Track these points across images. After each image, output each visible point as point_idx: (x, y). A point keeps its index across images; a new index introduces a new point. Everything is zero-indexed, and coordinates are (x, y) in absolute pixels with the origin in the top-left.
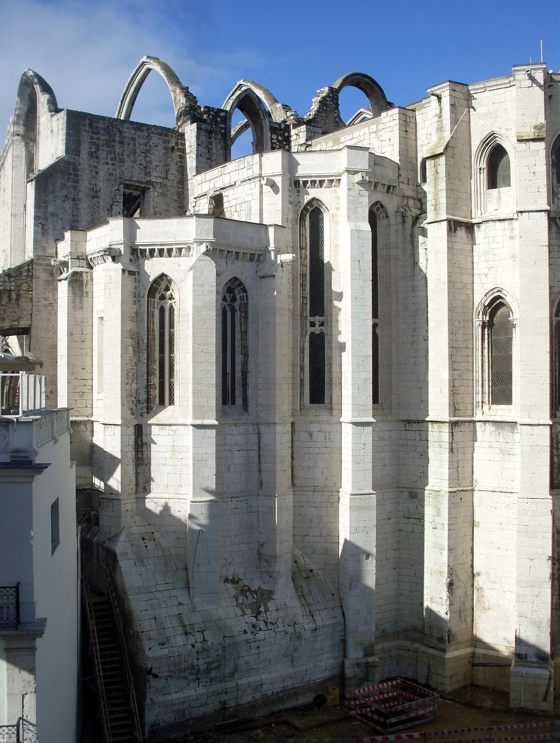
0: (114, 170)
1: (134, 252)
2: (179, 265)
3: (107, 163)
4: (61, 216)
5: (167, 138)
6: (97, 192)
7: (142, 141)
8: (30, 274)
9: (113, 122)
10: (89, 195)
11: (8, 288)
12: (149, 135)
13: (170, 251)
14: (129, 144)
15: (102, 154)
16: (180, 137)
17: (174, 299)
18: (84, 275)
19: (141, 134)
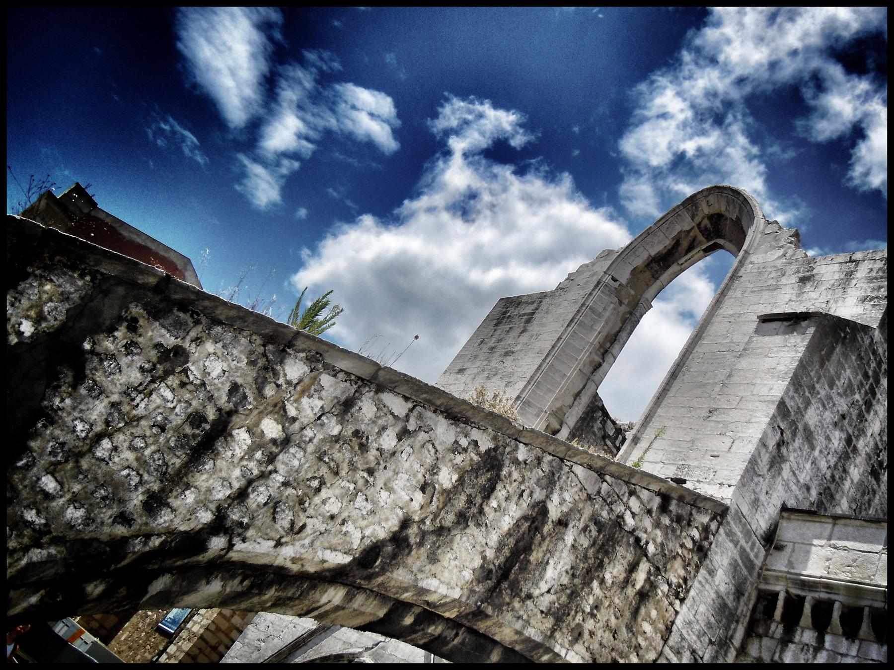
4: (817, 453)
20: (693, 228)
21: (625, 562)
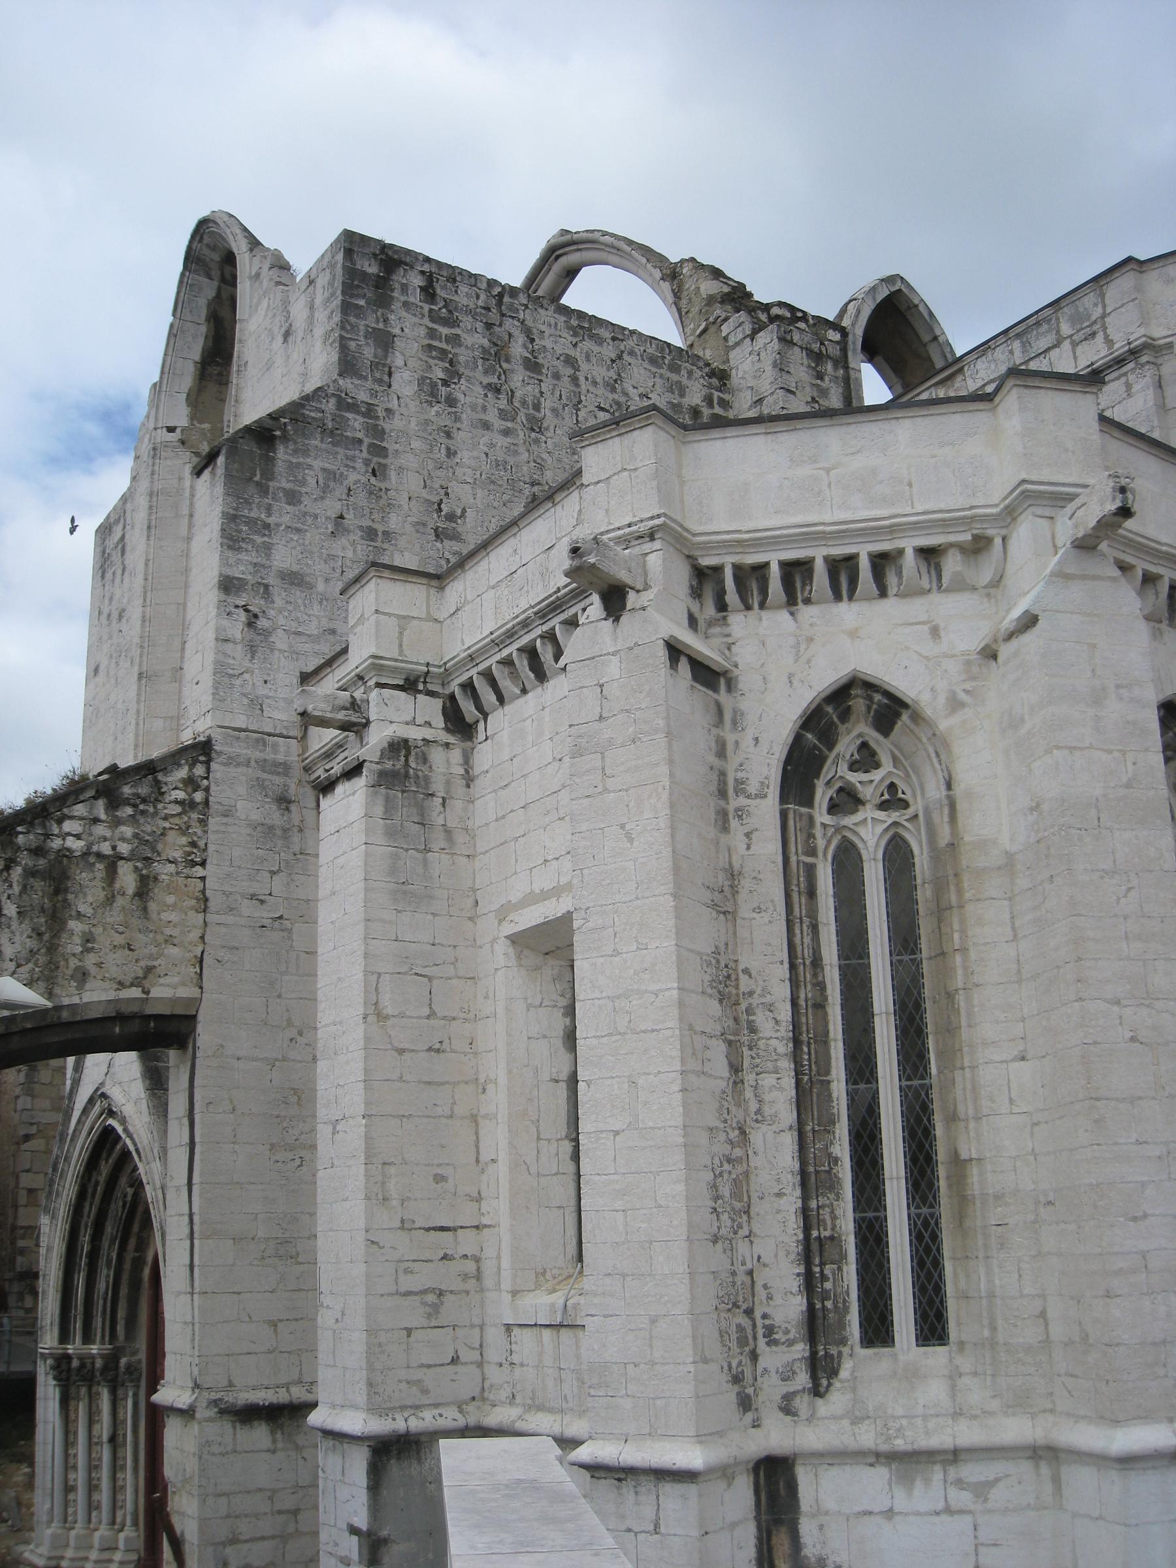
0: (512, 450)
1: (700, 583)
2: (935, 632)
3: (486, 426)
4: (321, 587)
5: (674, 377)
6: (451, 517)
7: (602, 373)
8: (199, 796)
9: (501, 296)
10: (424, 525)
11: (106, 848)
12: (620, 357)
13: (882, 562)
14: (557, 376)
15: (470, 392)
16: (715, 381)
17: (905, 805)
18: (437, 756)
19: (596, 349)
20: (219, 289)
21: (98, 883)
